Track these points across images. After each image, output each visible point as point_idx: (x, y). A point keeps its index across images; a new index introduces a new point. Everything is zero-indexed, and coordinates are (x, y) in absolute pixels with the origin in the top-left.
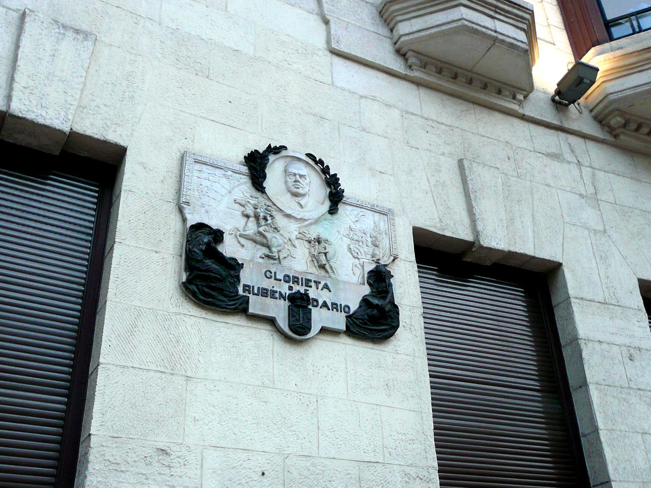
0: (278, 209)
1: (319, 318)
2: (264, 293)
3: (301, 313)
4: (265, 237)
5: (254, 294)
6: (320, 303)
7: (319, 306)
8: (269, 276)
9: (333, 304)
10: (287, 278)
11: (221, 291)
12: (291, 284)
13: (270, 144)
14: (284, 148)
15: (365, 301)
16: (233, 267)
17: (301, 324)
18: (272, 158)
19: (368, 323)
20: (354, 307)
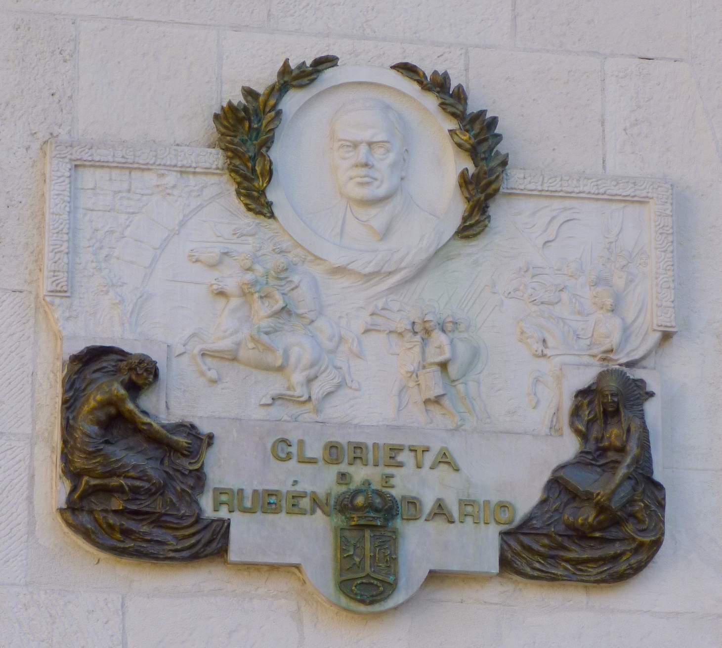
0: (310, 258)
1: (420, 546)
2: (268, 502)
3: (368, 545)
4: (269, 349)
5: (245, 510)
6: (428, 504)
7: (424, 517)
8: (283, 456)
9: (464, 503)
10: (333, 452)
11: (158, 521)
12: (344, 467)
13: (287, 61)
14: (326, 62)
15: (558, 484)
16: (183, 449)
17: (368, 576)
18: (292, 101)
19: (567, 543)
20: (526, 497)
